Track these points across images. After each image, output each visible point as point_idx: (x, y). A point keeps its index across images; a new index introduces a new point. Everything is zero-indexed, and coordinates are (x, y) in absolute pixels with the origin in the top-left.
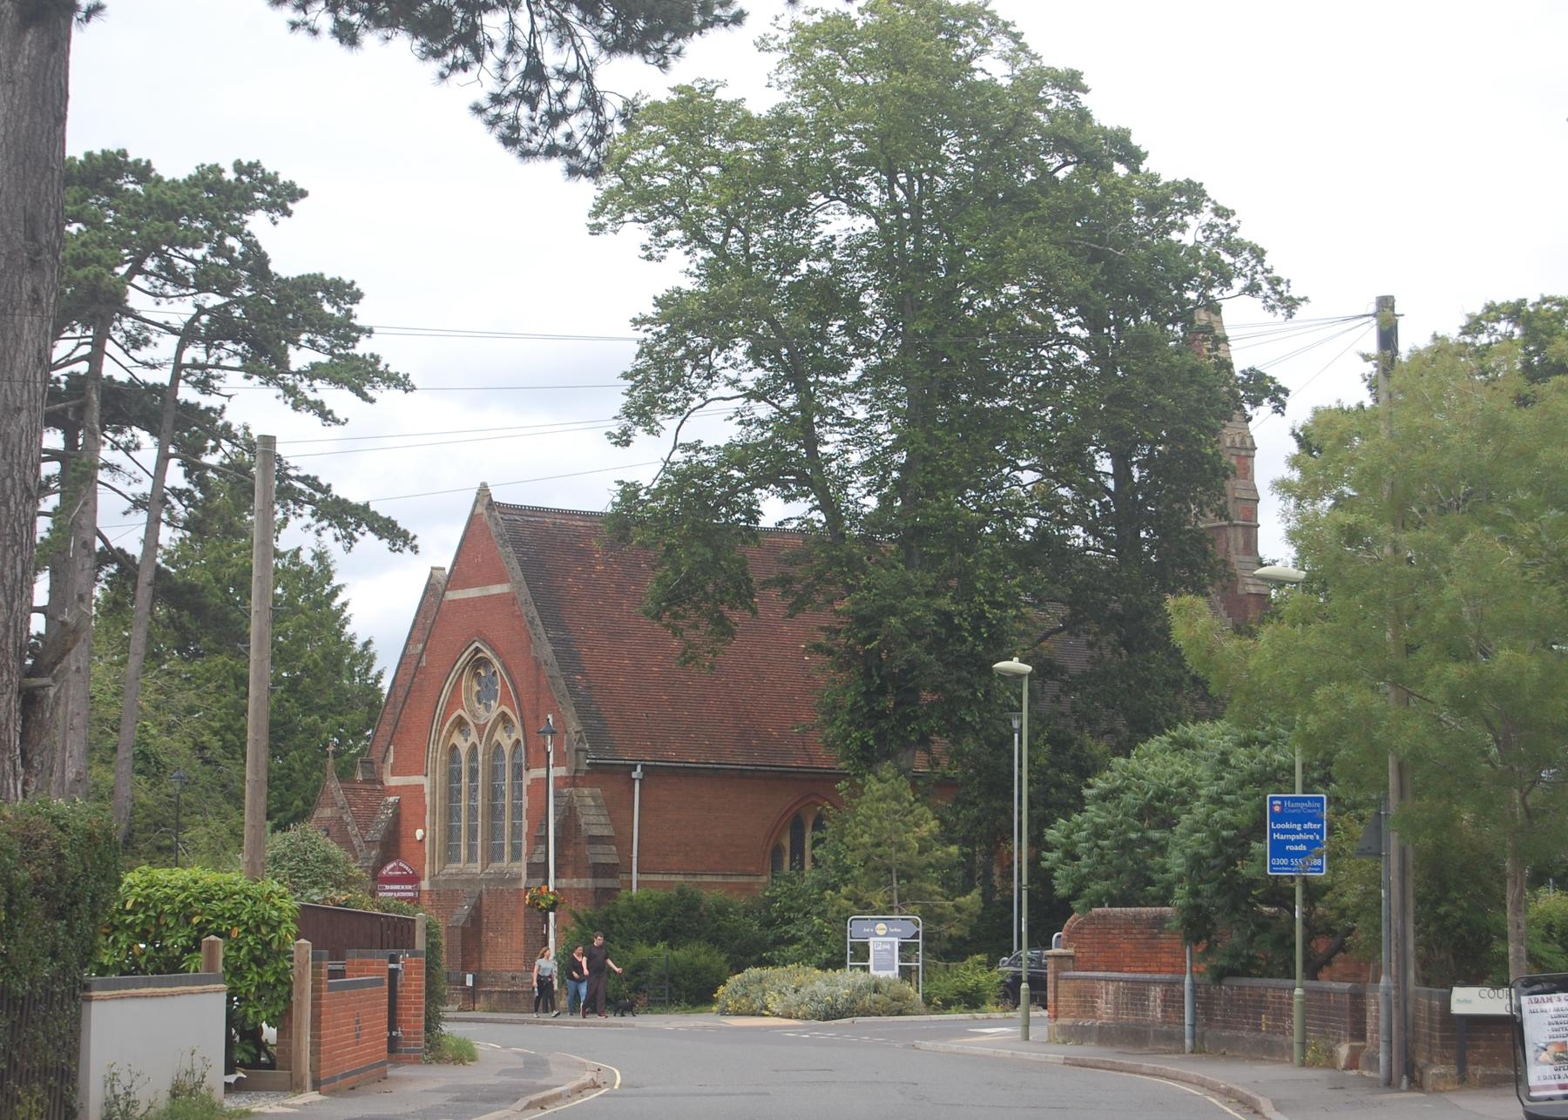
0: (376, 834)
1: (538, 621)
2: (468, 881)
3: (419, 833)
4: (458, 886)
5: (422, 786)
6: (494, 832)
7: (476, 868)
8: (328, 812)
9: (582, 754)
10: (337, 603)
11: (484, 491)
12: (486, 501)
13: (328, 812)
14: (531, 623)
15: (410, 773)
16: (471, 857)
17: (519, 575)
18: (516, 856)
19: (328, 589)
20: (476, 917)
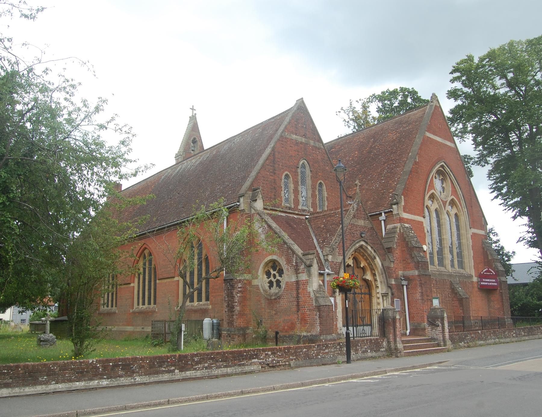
4: (446, 278)
15: (414, 214)
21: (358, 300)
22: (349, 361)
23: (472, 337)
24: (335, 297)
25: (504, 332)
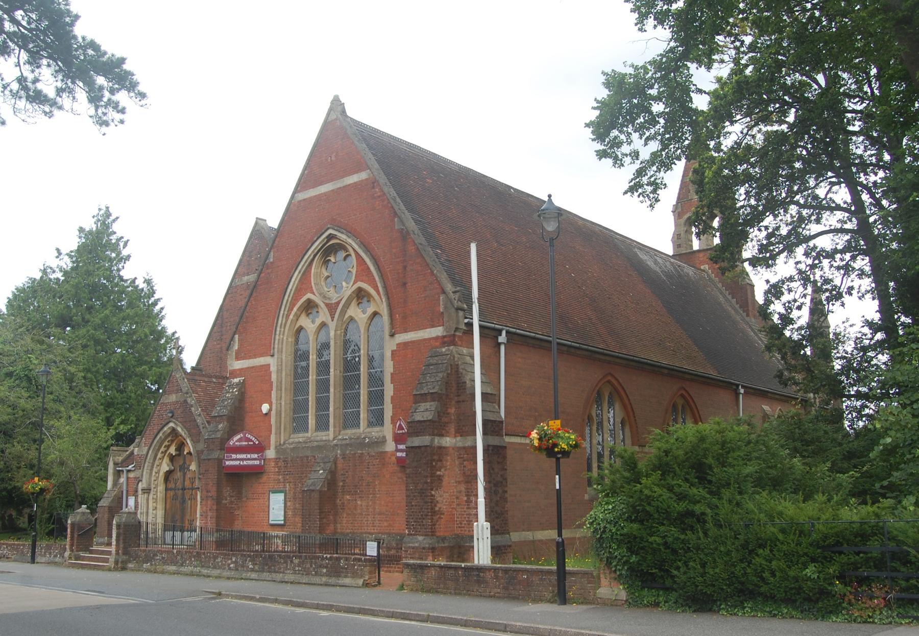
0: (222, 408)
1: (398, 200)
2: (319, 448)
3: (265, 408)
4: (309, 453)
5: (269, 365)
6: (350, 400)
7: (329, 435)
8: (173, 398)
9: (461, 313)
10: (157, 308)
11: (337, 105)
12: (340, 109)
13: (173, 398)
14: (395, 200)
15: (255, 356)
16: (322, 424)
17: (377, 166)
18: (377, 419)
19: (152, 299)
20: (332, 481)
21: (187, 497)
22: (33, 561)
23: (163, 558)
24: (136, 497)
25: (215, 558)
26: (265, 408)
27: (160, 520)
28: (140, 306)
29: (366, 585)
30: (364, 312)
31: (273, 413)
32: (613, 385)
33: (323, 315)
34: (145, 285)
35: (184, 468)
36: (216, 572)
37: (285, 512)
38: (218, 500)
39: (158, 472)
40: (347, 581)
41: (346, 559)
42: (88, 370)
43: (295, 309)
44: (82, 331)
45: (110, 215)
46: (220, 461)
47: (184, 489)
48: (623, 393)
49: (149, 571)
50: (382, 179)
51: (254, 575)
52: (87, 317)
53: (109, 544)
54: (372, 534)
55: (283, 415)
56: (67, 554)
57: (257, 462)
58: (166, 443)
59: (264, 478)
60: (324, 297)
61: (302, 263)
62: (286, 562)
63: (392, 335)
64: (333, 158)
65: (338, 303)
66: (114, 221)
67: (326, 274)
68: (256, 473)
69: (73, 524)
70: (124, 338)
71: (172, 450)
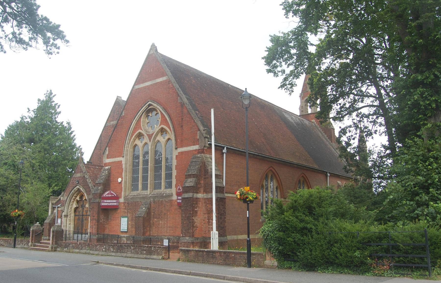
0: (100, 180)
1: (180, 89)
2: (144, 198)
3: (120, 180)
4: (138, 200)
5: (122, 161)
6: (157, 177)
8: (79, 175)
9: (207, 139)
10: (72, 135)
11: (154, 48)
12: (155, 49)
13: (79, 175)
14: (178, 89)
15: (116, 157)
16: (145, 187)
17: (170, 74)
18: (169, 185)
19: (70, 131)
20: (148, 213)
21: (84, 219)
22: (14, 247)
24: (61, 219)
25: (96, 246)
26: (120, 180)
27: (72, 229)
28: (65, 133)
29: (163, 258)
30: (164, 138)
31: (123, 182)
32: (272, 171)
33: (146, 139)
34: (67, 125)
35: (83, 206)
36: (97, 252)
37: (128, 226)
38: (98, 221)
39: (71, 208)
40: (155, 257)
41: (155, 247)
42: (41, 162)
43: (134, 137)
44: (39, 145)
45: (52, 94)
46: (99, 203)
47: (83, 215)
48: (277, 176)
49: (66, 252)
50: (173, 80)
51: (113, 254)
52: (41, 138)
53: (49, 240)
54: (166, 236)
55: (127, 183)
56: (30, 244)
57: (116, 204)
58: (75, 195)
59: (119, 211)
60: (147, 131)
61: (137, 116)
62: (128, 248)
63: (176, 149)
64: (152, 71)
65: (153, 134)
66: (54, 96)
67: (148, 121)
68: (115, 209)
69: (33, 231)
70: (57, 148)
71: (78, 198)
